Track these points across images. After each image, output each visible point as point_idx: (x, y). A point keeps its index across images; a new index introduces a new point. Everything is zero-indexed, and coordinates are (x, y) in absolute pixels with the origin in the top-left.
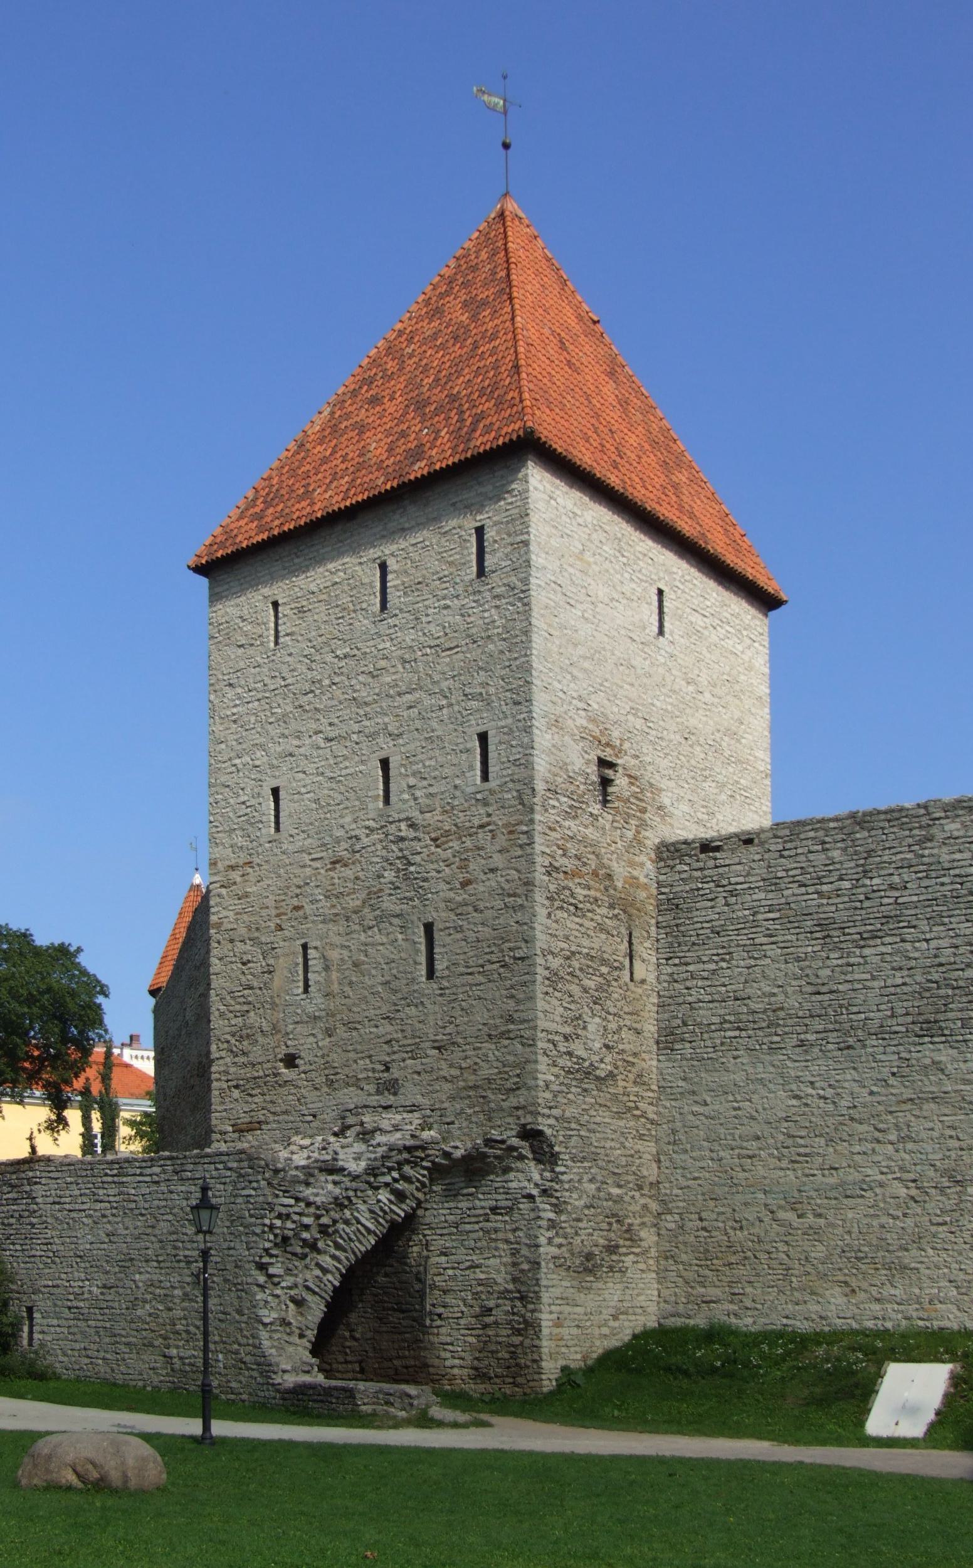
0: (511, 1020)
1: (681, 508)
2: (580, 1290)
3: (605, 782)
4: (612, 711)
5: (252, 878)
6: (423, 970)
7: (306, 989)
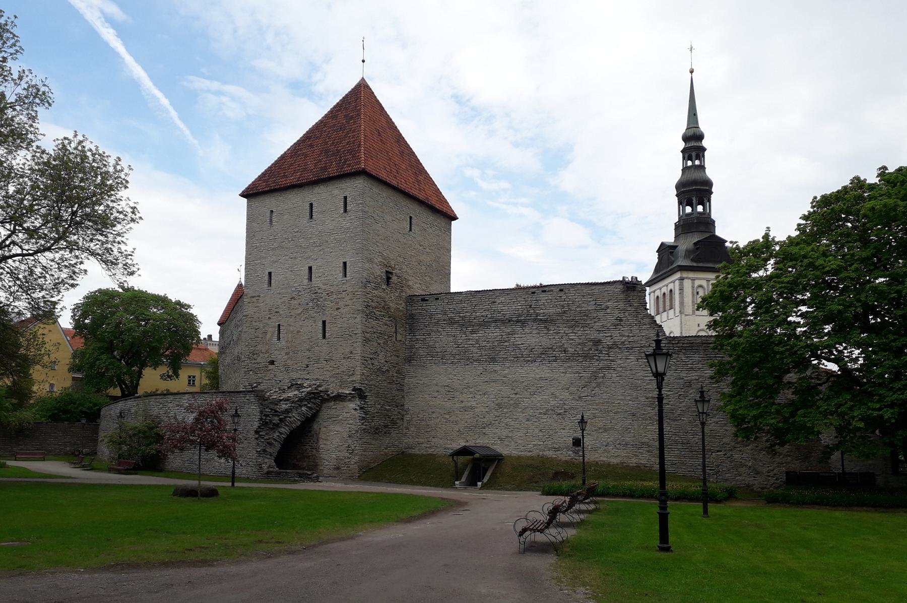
0: (351, 353)
1: (420, 190)
2: (373, 439)
3: (388, 279)
4: (392, 256)
5: (261, 301)
6: (321, 335)
7: (279, 339)
